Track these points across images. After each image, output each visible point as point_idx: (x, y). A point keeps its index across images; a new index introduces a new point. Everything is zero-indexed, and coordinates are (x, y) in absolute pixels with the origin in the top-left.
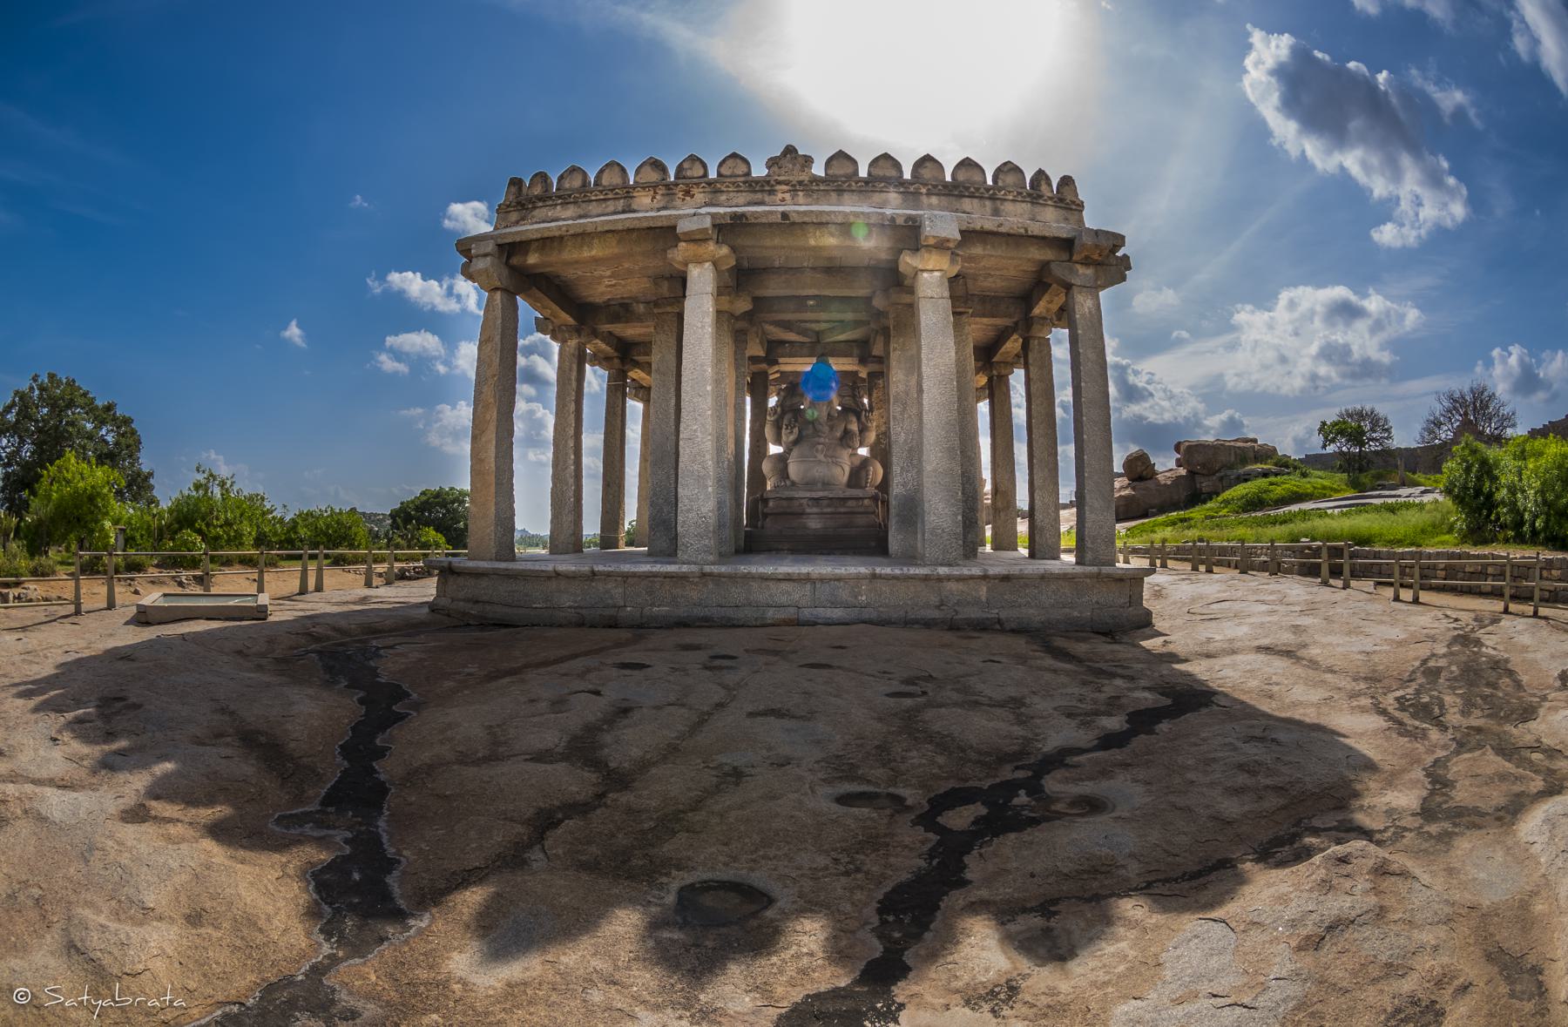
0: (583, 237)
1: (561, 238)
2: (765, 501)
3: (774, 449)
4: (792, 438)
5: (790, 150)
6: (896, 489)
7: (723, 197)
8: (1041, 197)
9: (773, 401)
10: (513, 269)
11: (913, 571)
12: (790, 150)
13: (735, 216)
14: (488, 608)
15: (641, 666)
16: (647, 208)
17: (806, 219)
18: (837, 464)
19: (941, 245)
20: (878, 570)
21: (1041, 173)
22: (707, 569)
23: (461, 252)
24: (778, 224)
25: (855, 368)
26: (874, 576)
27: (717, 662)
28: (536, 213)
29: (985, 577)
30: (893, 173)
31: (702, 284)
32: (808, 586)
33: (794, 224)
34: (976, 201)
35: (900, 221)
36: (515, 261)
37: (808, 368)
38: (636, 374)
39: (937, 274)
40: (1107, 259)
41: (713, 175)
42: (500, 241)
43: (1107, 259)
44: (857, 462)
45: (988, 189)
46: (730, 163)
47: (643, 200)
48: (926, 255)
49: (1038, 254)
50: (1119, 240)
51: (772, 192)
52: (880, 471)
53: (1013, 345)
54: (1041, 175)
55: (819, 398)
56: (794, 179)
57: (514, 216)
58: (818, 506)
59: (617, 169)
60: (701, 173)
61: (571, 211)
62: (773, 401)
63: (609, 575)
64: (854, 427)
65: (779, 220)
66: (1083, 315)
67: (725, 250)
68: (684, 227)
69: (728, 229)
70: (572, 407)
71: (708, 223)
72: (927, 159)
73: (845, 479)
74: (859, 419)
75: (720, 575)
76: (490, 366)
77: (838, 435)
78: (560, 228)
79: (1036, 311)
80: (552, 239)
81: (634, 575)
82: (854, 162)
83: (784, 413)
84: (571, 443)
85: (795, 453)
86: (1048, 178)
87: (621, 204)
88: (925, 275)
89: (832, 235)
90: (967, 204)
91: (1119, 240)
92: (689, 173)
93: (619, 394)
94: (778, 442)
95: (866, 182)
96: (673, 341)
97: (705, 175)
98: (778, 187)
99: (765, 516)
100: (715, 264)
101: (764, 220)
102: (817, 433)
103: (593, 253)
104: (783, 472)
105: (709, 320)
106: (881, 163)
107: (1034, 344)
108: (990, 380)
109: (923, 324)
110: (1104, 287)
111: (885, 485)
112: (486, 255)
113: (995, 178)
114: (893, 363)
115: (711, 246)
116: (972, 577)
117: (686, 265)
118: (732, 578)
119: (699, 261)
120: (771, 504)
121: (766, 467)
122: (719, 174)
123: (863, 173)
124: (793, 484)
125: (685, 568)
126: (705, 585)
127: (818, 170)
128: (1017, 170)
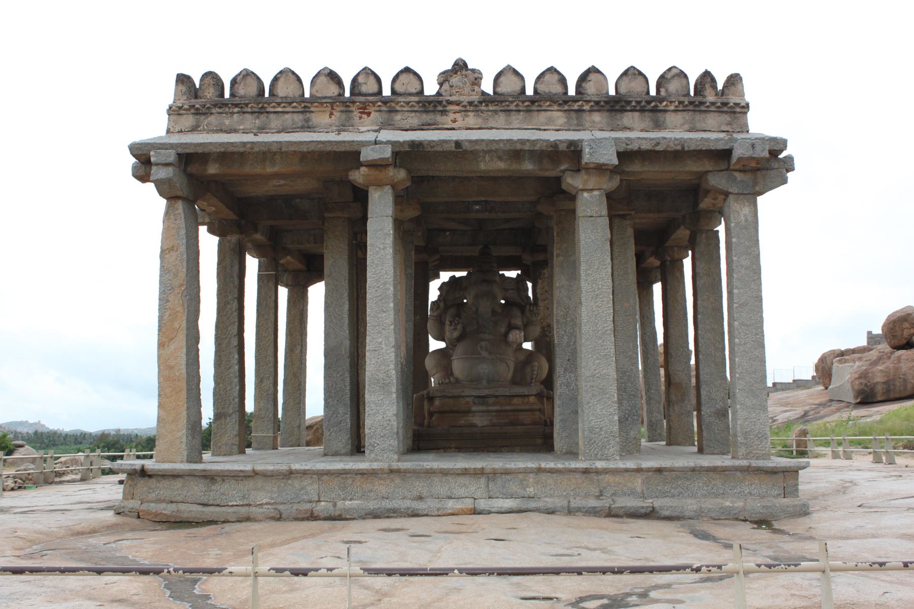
0: (267, 154)
2: (431, 399)
4: (456, 334)
5: (460, 66)
6: (560, 389)
7: (398, 117)
8: (702, 103)
9: (434, 294)
10: (190, 176)
11: (574, 465)
12: (460, 66)
13: (413, 144)
14: (182, 507)
15: (360, 542)
17: (477, 147)
19: (600, 169)
20: (543, 465)
22: (395, 465)
23: (134, 156)
24: (450, 152)
25: (519, 254)
26: (540, 470)
28: (212, 119)
29: (639, 470)
30: (557, 89)
32: (483, 480)
33: (466, 152)
34: (637, 114)
35: (563, 147)
36: (193, 169)
38: (287, 260)
39: (596, 193)
40: (769, 165)
41: (387, 92)
42: (180, 150)
43: (769, 165)
44: (522, 357)
45: (649, 102)
46: (404, 78)
47: (321, 118)
48: (586, 177)
49: (694, 167)
50: (782, 144)
51: (444, 112)
52: (546, 366)
53: (683, 233)
54: (707, 78)
56: (465, 99)
57: (188, 120)
58: (484, 404)
60: (374, 88)
61: (250, 121)
62: (434, 294)
63: (305, 473)
65: (453, 149)
66: (738, 224)
67: (402, 174)
68: (367, 155)
69: (407, 155)
70: (235, 305)
71: (387, 153)
72: (593, 70)
73: (510, 375)
74: (523, 312)
75: (406, 471)
76: (176, 275)
77: (503, 330)
78: (244, 144)
80: (233, 153)
81: (328, 473)
82: (522, 78)
83: (447, 308)
84: (235, 342)
85: (460, 349)
86: (713, 80)
87: (299, 118)
88: (585, 194)
89: (500, 158)
90: (629, 118)
91: (782, 144)
92: (364, 89)
93: (271, 285)
95: (532, 101)
98: (450, 107)
99: (431, 414)
100: (393, 187)
101: (439, 149)
103: (276, 169)
104: (447, 370)
105: (390, 241)
106: (547, 77)
107: (702, 238)
108: (663, 264)
109: (582, 242)
110: (761, 193)
111: (549, 383)
112: (167, 165)
113: (659, 85)
114: (557, 270)
115: (391, 172)
116: (627, 470)
117: (368, 187)
119: (380, 185)
120: (437, 402)
121: (429, 363)
122: (393, 91)
123: (530, 91)
124: (457, 381)
125: (375, 466)
126: (392, 481)
128: (683, 75)
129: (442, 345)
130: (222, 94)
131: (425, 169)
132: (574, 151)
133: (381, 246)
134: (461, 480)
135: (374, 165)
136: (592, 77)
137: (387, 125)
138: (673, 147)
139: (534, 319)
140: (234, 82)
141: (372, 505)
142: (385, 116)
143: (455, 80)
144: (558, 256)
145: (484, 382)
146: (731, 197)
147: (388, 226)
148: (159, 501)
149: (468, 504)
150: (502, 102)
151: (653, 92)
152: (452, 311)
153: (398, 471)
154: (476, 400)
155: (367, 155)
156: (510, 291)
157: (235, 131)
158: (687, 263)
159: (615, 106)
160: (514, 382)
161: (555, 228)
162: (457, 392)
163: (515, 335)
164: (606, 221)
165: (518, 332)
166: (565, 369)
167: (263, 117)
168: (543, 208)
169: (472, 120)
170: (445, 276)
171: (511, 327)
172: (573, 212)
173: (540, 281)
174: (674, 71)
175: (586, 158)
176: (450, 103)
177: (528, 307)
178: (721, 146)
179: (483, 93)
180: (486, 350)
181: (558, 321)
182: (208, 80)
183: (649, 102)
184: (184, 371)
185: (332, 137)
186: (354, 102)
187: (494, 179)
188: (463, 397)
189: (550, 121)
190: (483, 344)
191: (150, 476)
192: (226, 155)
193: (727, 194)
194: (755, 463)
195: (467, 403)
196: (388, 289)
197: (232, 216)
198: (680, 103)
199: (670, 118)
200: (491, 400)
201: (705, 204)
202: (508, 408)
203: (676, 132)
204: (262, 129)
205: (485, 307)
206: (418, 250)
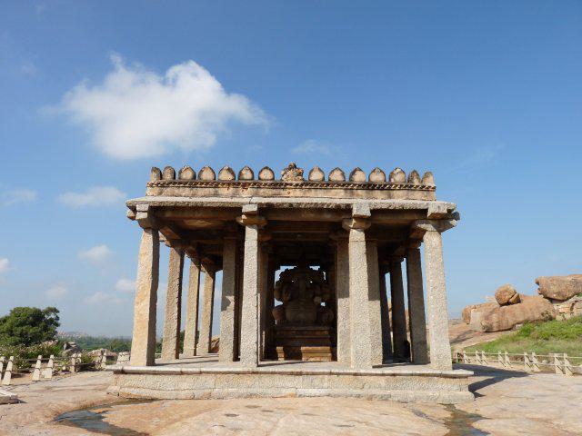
0: (197, 208)
1: (183, 207)
3: (277, 303)
7: (262, 191)
9: (277, 278)
14: (143, 390)
16: (225, 197)
19: (360, 218)
21: (415, 171)
27: (265, 413)
28: (168, 189)
29: (383, 375)
31: (251, 236)
41: (256, 178)
42: (151, 204)
49: (409, 218)
53: (401, 250)
57: (157, 190)
59: (209, 171)
61: (187, 191)
63: (208, 373)
67: (263, 219)
68: (246, 209)
69: (265, 210)
74: (321, 288)
75: (261, 373)
77: (311, 296)
79: (412, 236)
84: (176, 300)
87: (212, 190)
88: (354, 231)
90: (377, 193)
92: (245, 177)
94: (279, 300)
96: (233, 255)
97: (253, 179)
116: (376, 375)
118: (265, 373)
119: (251, 225)
120: (278, 333)
121: (274, 313)
123: (327, 180)
124: (288, 322)
125: (246, 369)
127: (306, 176)
129: (281, 303)
130: (175, 178)
131: (275, 218)
132: (348, 209)
134: (292, 377)
135: (248, 214)
136: (358, 173)
137: (256, 195)
138: (398, 207)
140: (180, 172)
141: (243, 391)
142: (255, 190)
143: (290, 173)
146: (427, 233)
147: (255, 244)
148: (131, 387)
149: (292, 391)
150: (312, 185)
151: (387, 180)
153: (257, 373)
155: (246, 209)
157: (181, 196)
158: (404, 264)
159: (369, 187)
161: (337, 244)
162: (288, 328)
163: (317, 299)
164: (364, 244)
167: (194, 189)
168: (332, 237)
169: (298, 192)
170: (283, 269)
172: (348, 238)
174: (398, 170)
175: (354, 213)
176: (287, 184)
178: (422, 207)
179: (303, 180)
182: (168, 170)
183: (385, 185)
184: (148, 317)
185: (229, 200)
186: (239, 183)
187: (308, 224)
189: (337, 194)
191: (126, 373)
192: (176, 208)
193: (424, 231)
194: (444, 372)
197: (177, 237)
198: (401, 186)
199: (395, 193)
201: (413, 236)
203: (399, 200)
204: (193, 195)
206: (270, 256)
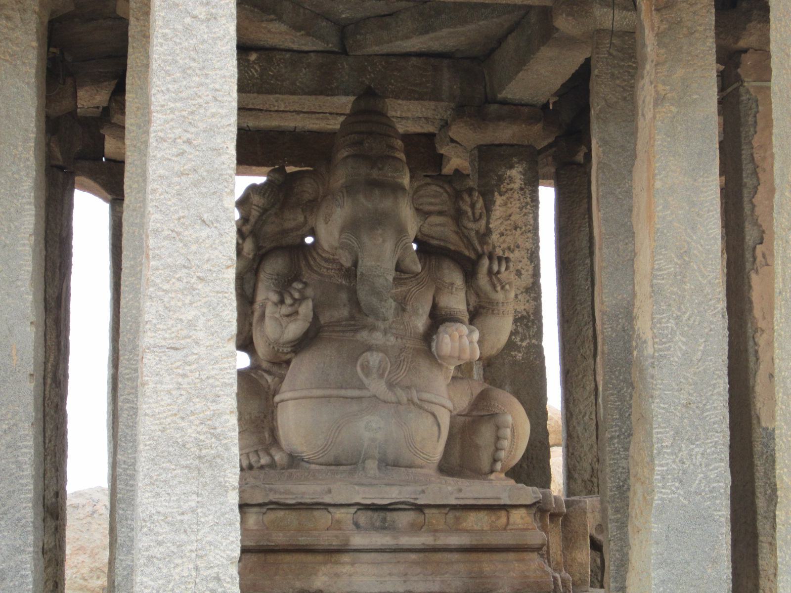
4: (294, 330)
18: (421, 406)
37: (334, 124)
55: (379, 220)
58: (384, 528)
64: (456, 301)
73: (437, 450)
77: (421, 323)
102: (359, 316)
124: (294, 460)
133: (201, 12)
139: (500, 296)
144: (659, 100)
145: (372, 465)
152: (274, 266)
154: (363, 518)
156: (435, 219)
160: (447, 468)
165: (464, 329)
166: (677, 433)
171: (439, 318)
173: (499, 200)
177: (486, 262)
180: (381, 376)
181: (656, 291)
188: (326, 506)
190: (374, 359)
195: (337, 525)
196: (217, 151)
200: (404, 519)
202: (454, 540)
205: (381, 256)
